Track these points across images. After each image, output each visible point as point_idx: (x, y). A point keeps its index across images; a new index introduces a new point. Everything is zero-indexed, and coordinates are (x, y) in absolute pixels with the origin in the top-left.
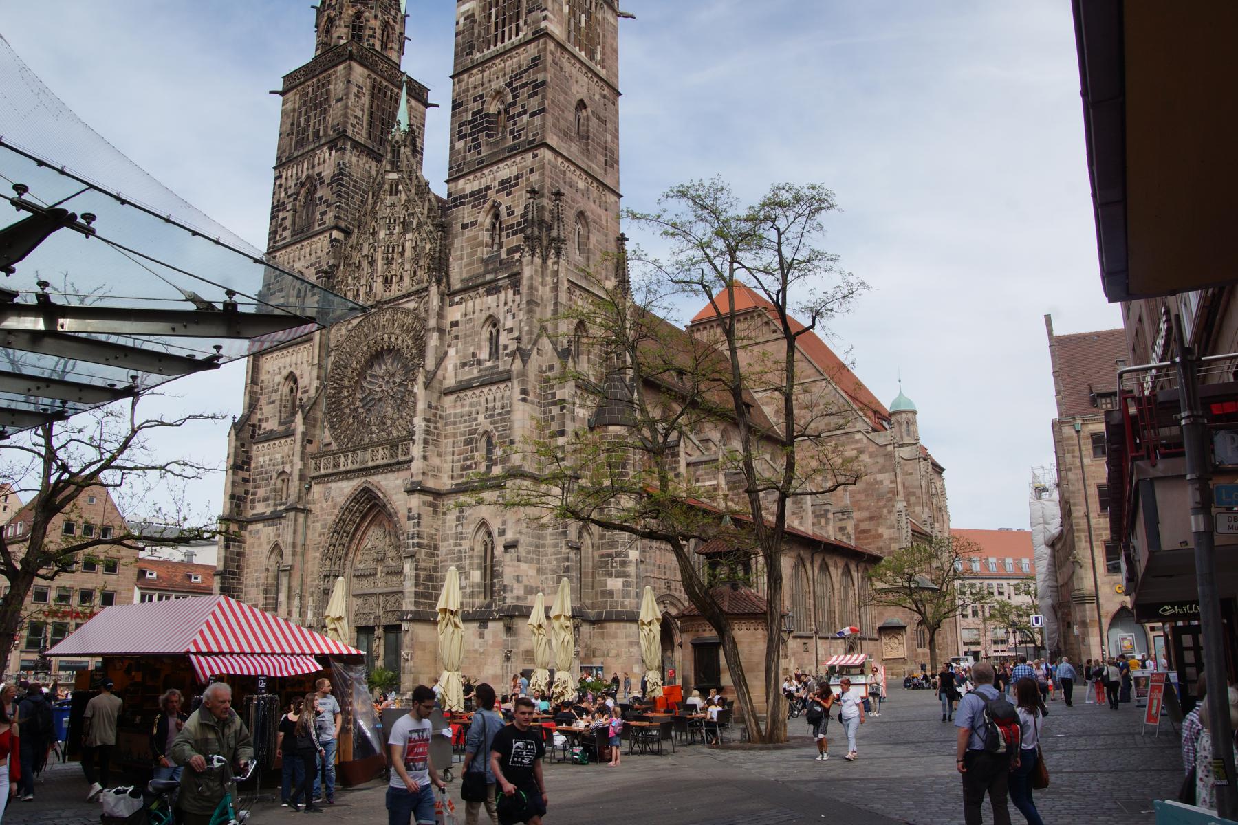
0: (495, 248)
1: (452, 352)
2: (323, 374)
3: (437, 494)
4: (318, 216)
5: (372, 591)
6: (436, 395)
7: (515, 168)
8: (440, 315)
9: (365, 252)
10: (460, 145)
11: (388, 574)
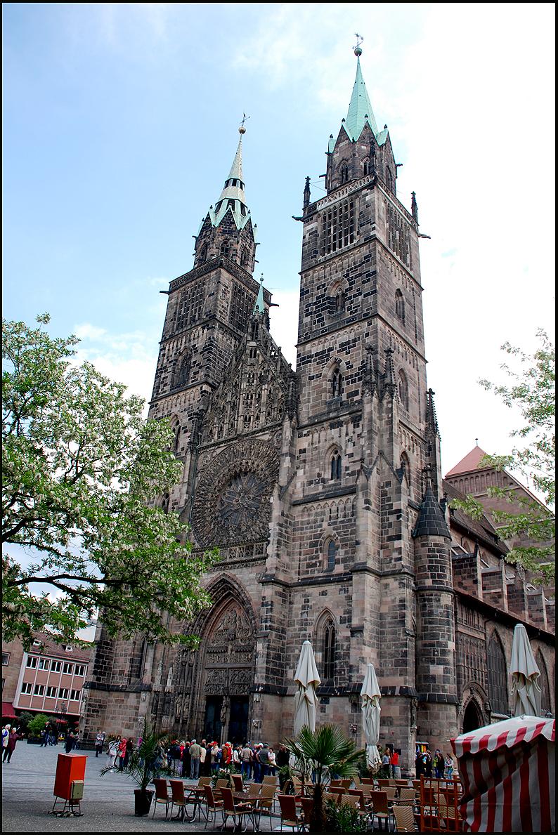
0: (336, 393)
1: (300, 472)
2: (191, 490)
3: (286, 586)
4: (192, 375)
5: (222, 666)
6: (288, 506)
7: (353, 334)
8: (292, 444)
9: (229, 399)
10: (307, 320)
11: (237, 652)
